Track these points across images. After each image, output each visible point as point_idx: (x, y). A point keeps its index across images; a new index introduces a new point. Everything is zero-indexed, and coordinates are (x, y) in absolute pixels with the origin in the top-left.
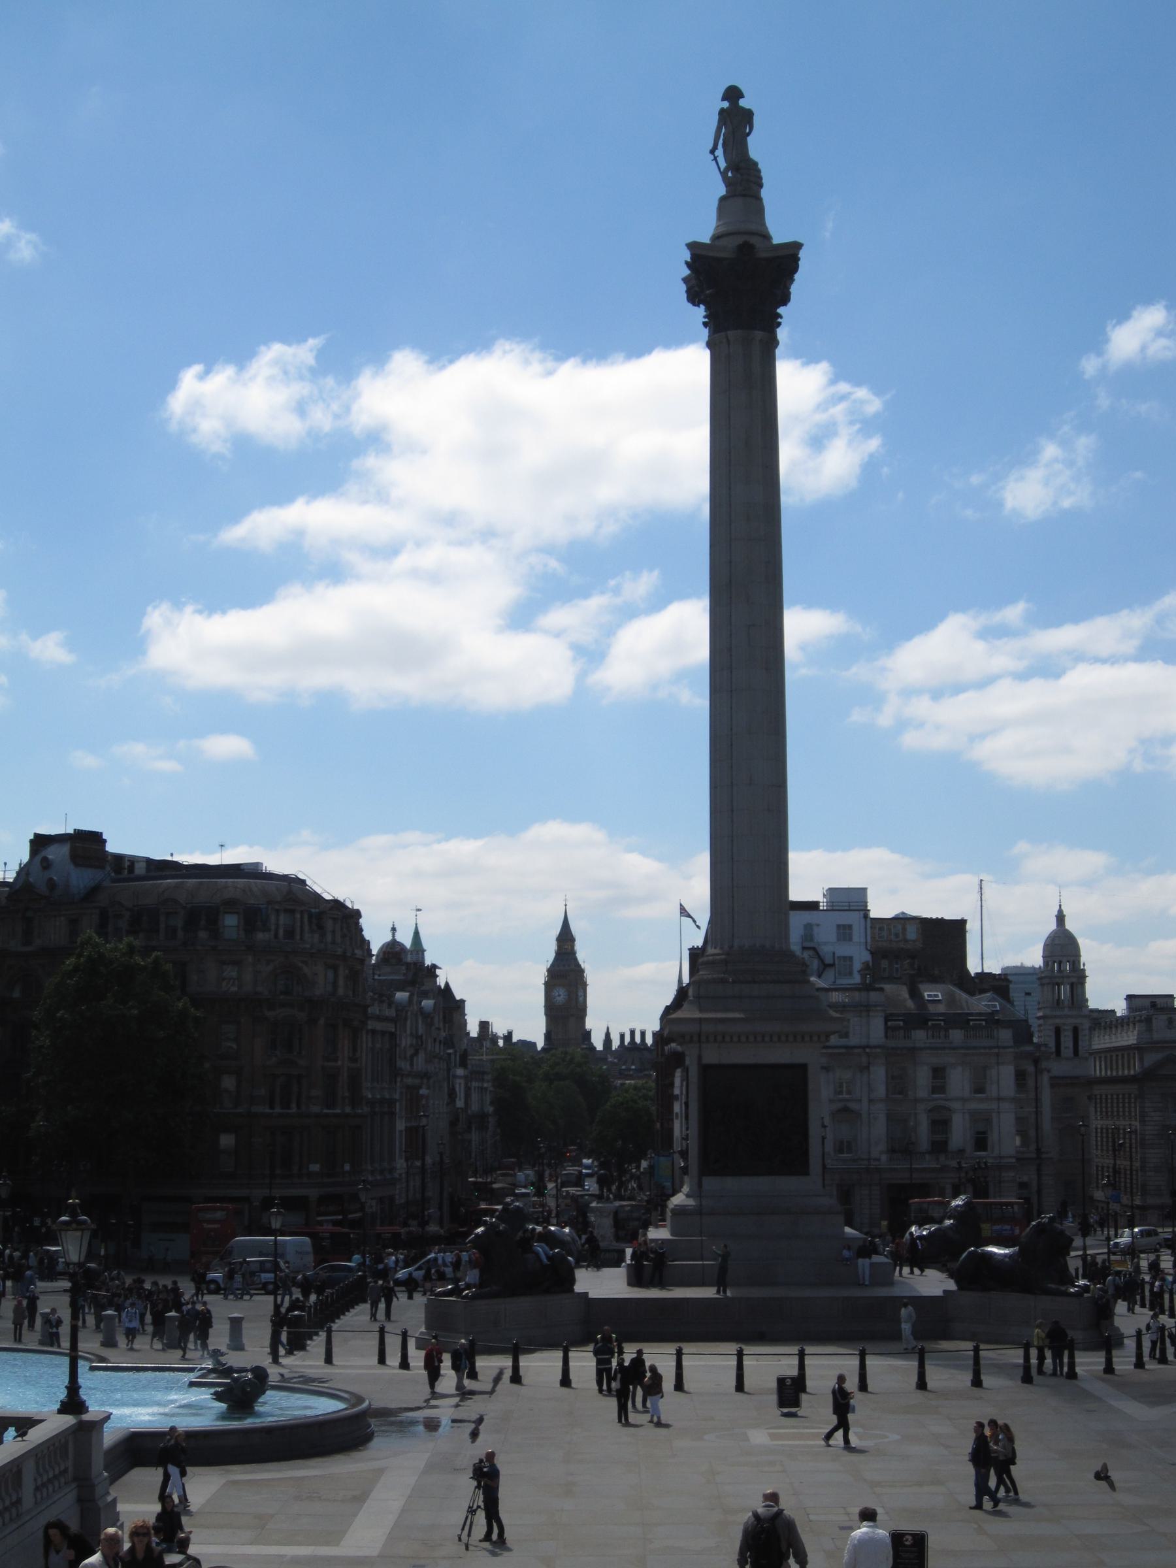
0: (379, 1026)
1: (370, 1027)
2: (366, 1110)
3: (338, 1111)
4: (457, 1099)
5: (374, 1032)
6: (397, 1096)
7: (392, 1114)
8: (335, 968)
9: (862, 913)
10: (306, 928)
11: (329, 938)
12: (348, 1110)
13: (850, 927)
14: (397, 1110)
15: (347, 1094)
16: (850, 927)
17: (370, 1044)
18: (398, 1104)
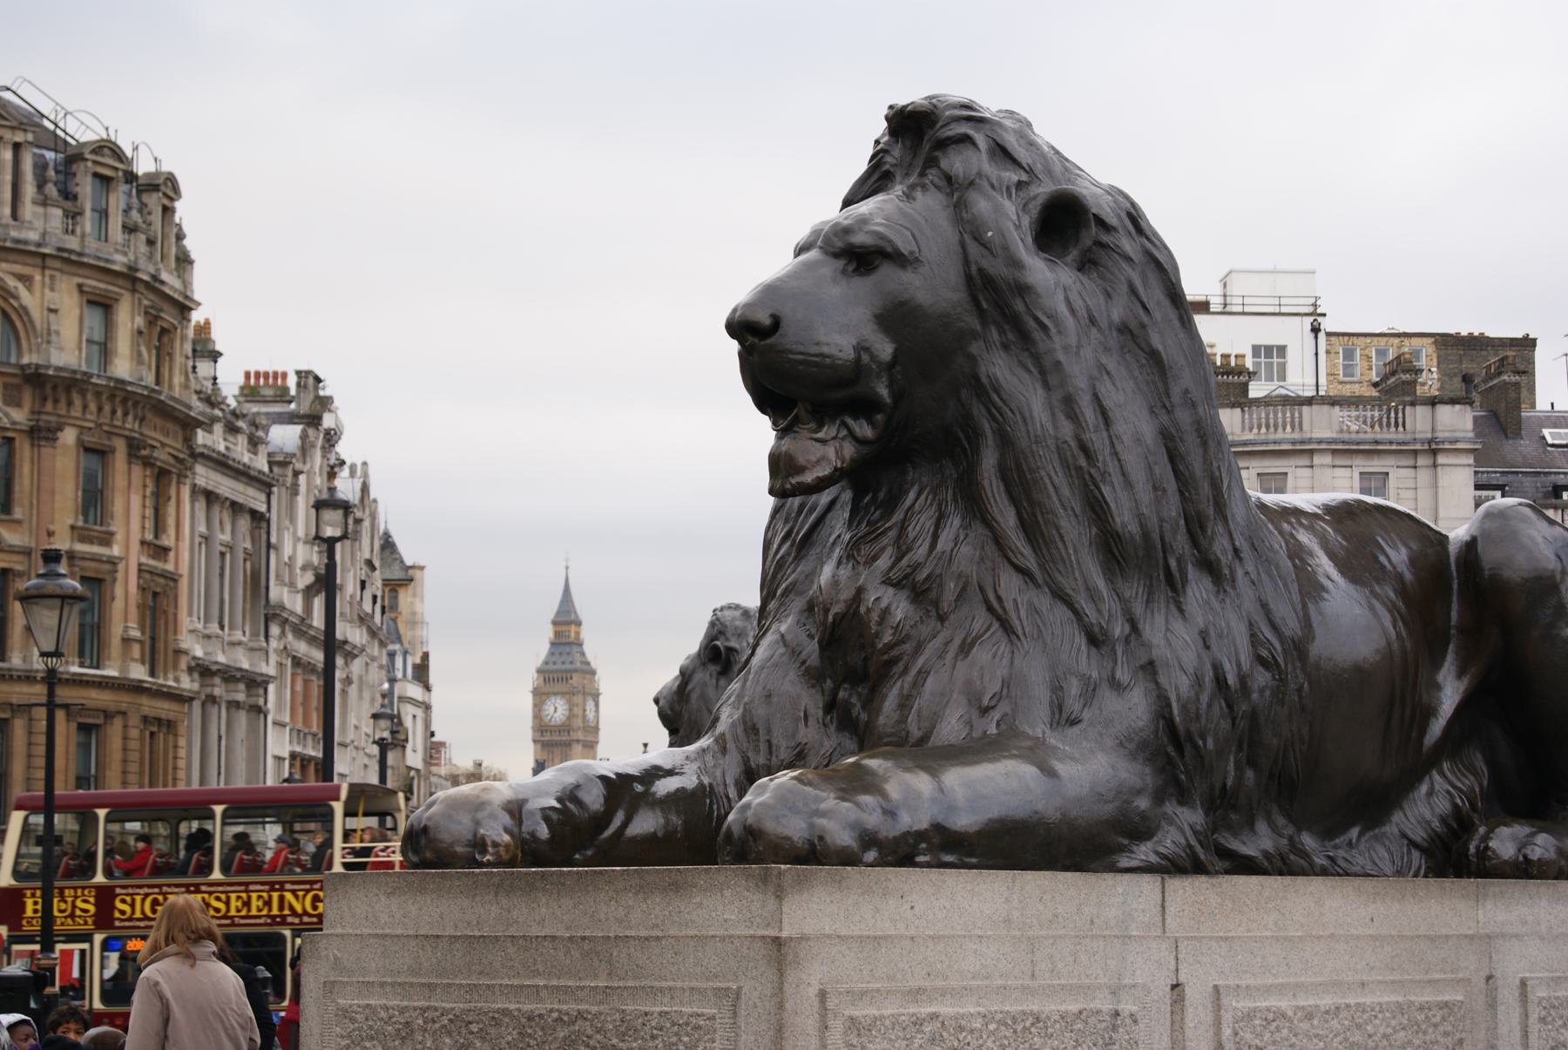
0: (226, 486)
1: (201, 482)
2: (187, 684)
3: (111, 672)
4: (409, 747)
5: (210, 497)
6: (270, 670)
7: (258, 711)
8: (103, 305)
9: (1311, 319)
10: (29, 190)
11: (88, 223)
12: (139, 672)
13: (1282, 350)
14: (271, 704)
15: (136, 634)
16: (1282, 350)
17: (202, 528)
18: (271, 688)
